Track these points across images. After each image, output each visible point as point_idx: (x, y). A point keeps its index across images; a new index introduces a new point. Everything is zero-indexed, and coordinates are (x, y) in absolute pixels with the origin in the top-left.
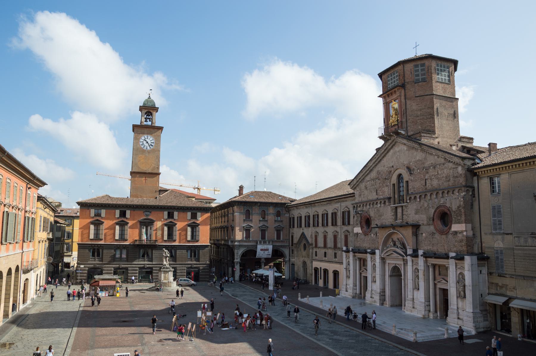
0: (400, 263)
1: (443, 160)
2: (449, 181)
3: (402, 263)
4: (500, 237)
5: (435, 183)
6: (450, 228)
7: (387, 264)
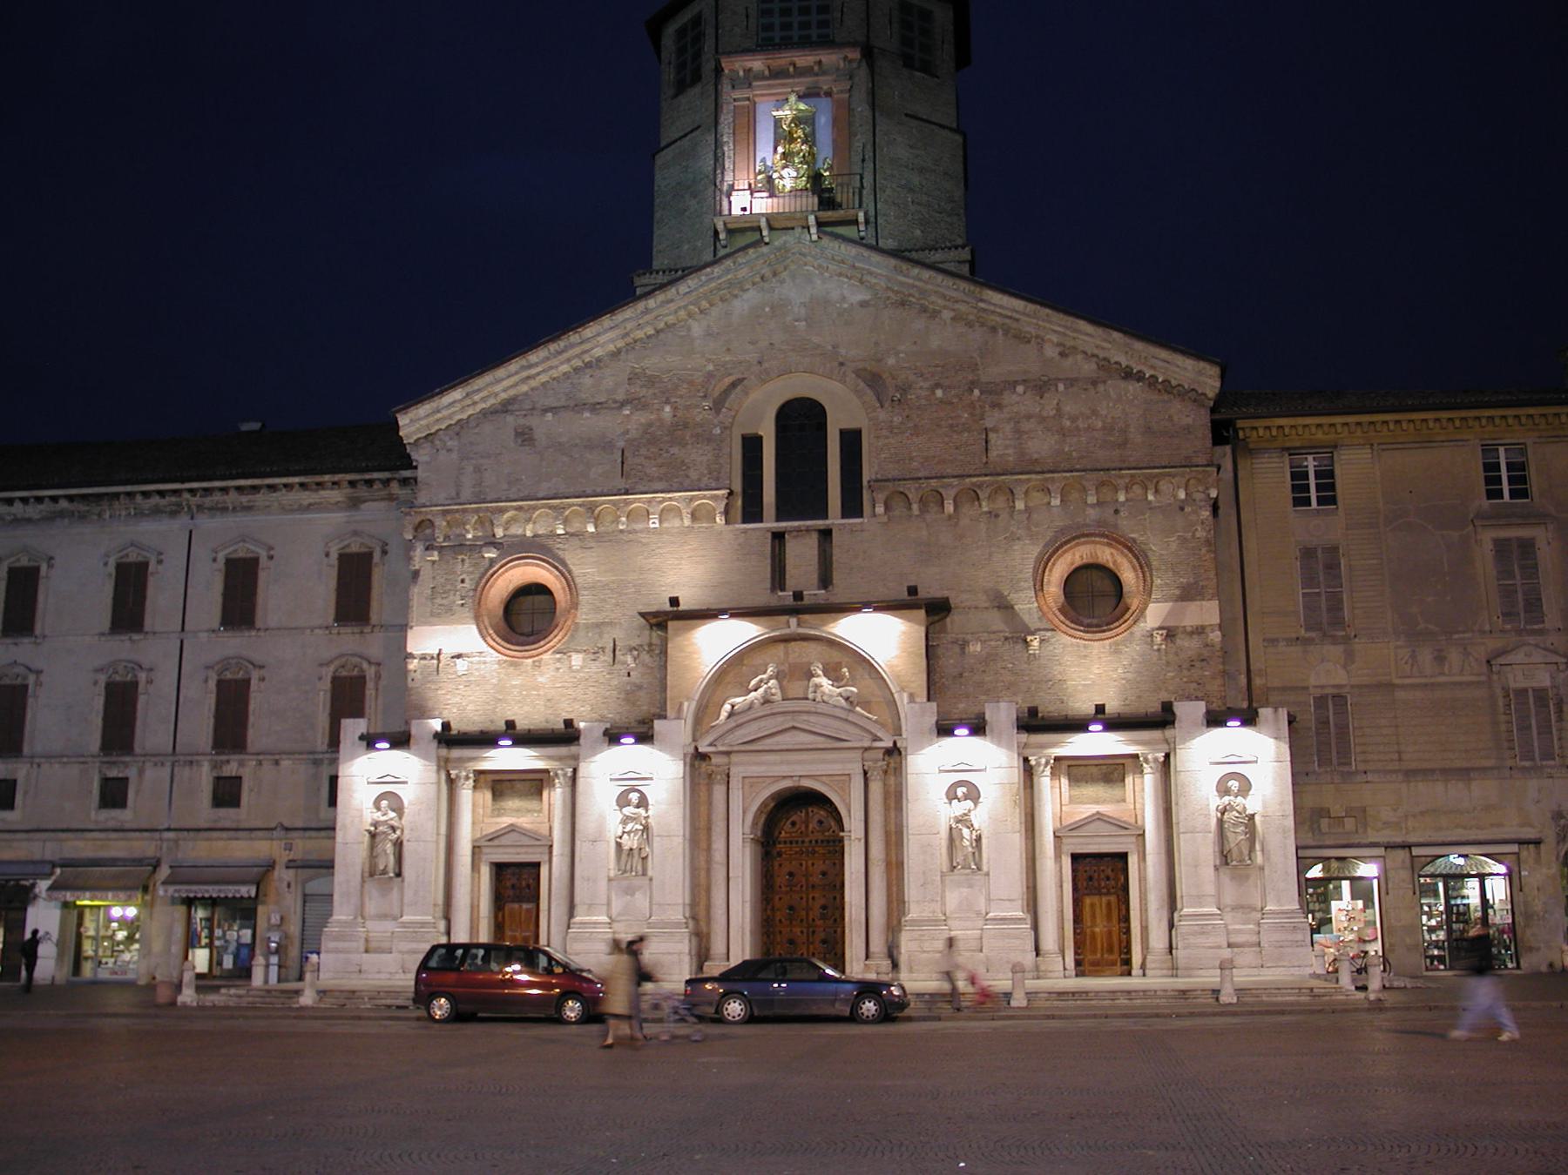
2: (1123, 444)
4: (1336, 651)
5: (1041, 445)
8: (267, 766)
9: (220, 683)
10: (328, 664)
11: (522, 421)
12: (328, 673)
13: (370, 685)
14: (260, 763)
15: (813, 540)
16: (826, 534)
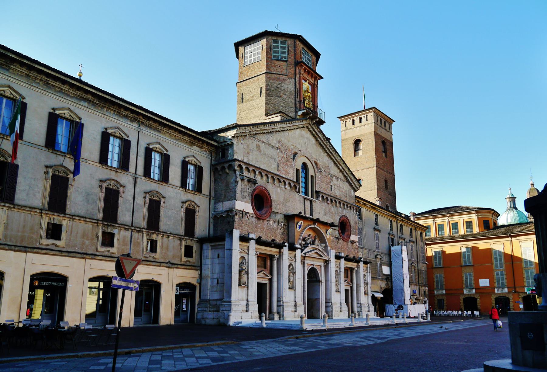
0: (318, 264)
1: (343, 177)
3: (322, 264)
6: (350, 237)
8: (165, 238)
9: (150, 200)
10: (185, 202)
11: (258, 143)
12: (185, 206)
13: (197, 214)
14: (163, 236)
15: (309, 202)
16: (311, 202)
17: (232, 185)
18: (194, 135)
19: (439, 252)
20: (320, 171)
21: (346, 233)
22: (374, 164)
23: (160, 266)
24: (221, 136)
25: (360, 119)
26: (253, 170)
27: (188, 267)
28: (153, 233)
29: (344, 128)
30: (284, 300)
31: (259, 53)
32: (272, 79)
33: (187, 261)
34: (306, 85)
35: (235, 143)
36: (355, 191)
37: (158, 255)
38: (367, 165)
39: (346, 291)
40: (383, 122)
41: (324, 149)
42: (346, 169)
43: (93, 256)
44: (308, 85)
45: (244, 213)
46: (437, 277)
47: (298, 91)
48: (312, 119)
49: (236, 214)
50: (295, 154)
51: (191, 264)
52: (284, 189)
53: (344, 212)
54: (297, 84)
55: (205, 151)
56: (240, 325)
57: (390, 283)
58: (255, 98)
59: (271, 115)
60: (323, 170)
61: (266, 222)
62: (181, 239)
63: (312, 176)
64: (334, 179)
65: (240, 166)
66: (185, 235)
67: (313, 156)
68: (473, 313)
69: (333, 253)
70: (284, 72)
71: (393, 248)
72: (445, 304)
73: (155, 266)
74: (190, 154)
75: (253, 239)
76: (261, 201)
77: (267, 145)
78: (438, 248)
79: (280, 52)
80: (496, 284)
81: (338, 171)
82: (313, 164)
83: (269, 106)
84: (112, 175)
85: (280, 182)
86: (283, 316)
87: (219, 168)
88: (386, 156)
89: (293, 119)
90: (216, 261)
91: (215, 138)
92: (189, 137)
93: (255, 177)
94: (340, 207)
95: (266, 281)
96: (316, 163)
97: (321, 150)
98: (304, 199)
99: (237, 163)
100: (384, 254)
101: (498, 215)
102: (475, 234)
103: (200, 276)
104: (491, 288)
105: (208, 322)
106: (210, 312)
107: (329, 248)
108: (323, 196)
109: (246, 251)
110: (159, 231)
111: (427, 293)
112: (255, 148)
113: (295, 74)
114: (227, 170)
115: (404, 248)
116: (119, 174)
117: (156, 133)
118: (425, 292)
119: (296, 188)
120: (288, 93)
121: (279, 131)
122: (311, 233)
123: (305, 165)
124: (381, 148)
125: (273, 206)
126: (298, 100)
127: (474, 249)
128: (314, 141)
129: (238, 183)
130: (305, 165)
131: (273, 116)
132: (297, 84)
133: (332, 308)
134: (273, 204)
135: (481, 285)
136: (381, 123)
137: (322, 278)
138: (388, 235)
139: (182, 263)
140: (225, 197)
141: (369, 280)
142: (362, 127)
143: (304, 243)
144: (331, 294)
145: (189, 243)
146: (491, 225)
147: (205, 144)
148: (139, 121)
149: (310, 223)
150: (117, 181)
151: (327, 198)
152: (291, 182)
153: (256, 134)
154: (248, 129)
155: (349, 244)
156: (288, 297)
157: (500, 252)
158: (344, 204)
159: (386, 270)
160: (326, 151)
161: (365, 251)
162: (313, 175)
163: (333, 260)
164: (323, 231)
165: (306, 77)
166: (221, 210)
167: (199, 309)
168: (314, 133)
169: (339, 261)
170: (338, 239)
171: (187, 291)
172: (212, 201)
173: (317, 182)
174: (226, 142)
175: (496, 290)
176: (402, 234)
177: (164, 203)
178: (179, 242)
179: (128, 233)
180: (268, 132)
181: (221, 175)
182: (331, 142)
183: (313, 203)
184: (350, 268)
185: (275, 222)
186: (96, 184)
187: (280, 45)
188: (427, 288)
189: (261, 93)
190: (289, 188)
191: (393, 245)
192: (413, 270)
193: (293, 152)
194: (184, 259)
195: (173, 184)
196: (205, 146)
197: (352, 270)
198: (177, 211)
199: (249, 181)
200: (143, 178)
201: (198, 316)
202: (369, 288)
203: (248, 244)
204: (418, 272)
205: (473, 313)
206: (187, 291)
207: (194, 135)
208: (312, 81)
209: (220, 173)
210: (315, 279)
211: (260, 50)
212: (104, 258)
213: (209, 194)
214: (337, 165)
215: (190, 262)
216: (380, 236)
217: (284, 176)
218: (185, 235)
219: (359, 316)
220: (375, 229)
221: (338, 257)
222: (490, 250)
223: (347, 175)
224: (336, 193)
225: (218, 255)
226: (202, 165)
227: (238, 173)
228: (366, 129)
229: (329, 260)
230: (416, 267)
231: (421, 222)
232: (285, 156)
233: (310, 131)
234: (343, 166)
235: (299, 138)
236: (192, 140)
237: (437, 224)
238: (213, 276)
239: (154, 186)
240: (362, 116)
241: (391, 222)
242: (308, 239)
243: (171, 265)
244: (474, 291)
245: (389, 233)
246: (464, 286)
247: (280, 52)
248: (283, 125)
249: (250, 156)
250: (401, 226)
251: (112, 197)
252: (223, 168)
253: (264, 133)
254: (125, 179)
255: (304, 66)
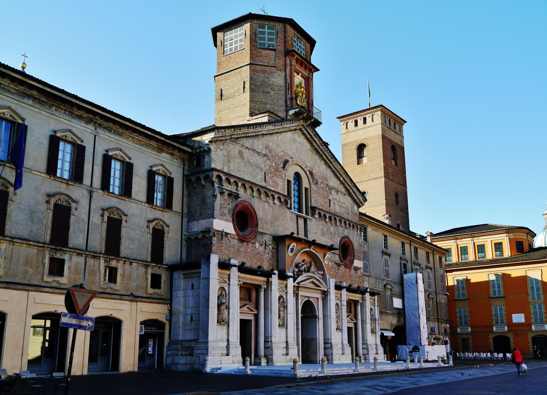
0: (315, 295)
1: (343, 190)
3: (319, 296)
4: (367, 278)
6: (353, 263)
7: (300, 297)
11: (240, 149)
12: (152, 225)
13: (166, 235)
14: (124, 263)
15: (303, 220)
16: (305, 220)
17: (208, 200)
18: (163, 139)
19: (462, 281)
20: (316, 183)
21: (348, 258)
22: (382, 173)
23: (121, 299)
24: (195, 141)
25: (365, 119)
26: (235, 182)
27: (155, 301)
28: (112, 259)
29: (345, 131)
30: (273, 340)
31: (241, 40)
32: (258, 71)
33: (154, 293)
34: (298, 79)
35: (213, 149)
36: (359, 206)
37: (118, 286)
38: (374, 176)
39: (349, 329)
40: (392, 123)
41: (321, 156)
42: (348, 180)
43: (39, 288)
44: (301, 78)
45: (224, 233)
46: (460, 312)
47: (289, 85)
48: (306, 119)
49: (214, 236)
50: (286, 162)
51: (158, 297)
52: (272, 204)
53: (346, 232)
54: (288, 78)
55: (177, 159)
56: (219, 371)
57: (402, 319)
58: (237, 94)
59: (257, 115)
60: (320, 181)
61: (250, 245)
62: (146, 266)
63: (306, 189)
64: (333, 192)
65: (219, 177)
66: (152, 261)
67: (308, 164)
68: (505, 355)
69: (332, 282)
70: (272, 63)
71: (405, 276)
72: (471, 345)
73: (114, 299)
74: (159, 162)
75: (235, 266)
76: (244, 219)
77: (251, 152)
78: (461, 275)
79: (266, 39)
80: (533, 320)
81: (338, 182)
82: (308, 173)
83: (254, 104)
84: (63, 188)
85: (267, 195)
86: (272, 360)
87: (193, 179)
88: (396, 164)
89: (283, 120)
90: (190, 293)
91: (188, 143)
92: (156, 142)
93: (237, 190)
94: (341, 226)
95: (251, 317)
96: (311, 173)
97: (317, 157)
98: (297, 216)
99: (215, 174)
100: (394, 283)
101: (534, 235)
102: (506, 258)
103: (170, 311)
104: (527, 324)
105: (180, 368)
106: (182, 355)
107: (328, 276)
108: (319, 214)
109: (227, 280)
110: (119, 257)
111: (448, 331)
112: (237, 155)
113: (285, 65)
114: (203, 182)
115: (420, 276)
116: (71, 187)
117: (116, 137)
118: (445, 330)
119: (287, 203)
120: (276, 88)
121: (266, 134)
122: (306, 258)
123: (297, 176)
124: (391, 154)
125: (259, 225)
126: (289, 96)
127: (505, 276)
128: (308, 146)
129: (216, 198)
130: (297, 176)
131: (259, 116)
132: (288, 78)
133: (332, 350)
134: (259, 223)
135: (514, 321)
136: (390, 125)
137: (320, 313)
138: (399, 261)
139: (148, 296)
140: (201, 215)
141: (377, 315)
142: (366, 129)
143: (297, 270)
144: (331, 333)
145: (157, 271)
146: (526, 247)
147: (176, 151)
148: (95, 123)
149: (304, 246)
150: (68, 196)
151: (325, 215)
152: (281, 196)
153: (238, 138)
154: (228, 132)
155: (352, 271)
156: (278, 336)
157: (537, 280)
158: (345, 223)
159: (397, 303)
160: (323, 158)
161: (372, 280)
162: (308, 187)
163: (333, 291)
164: (320, 256)
165: (298, 69)
166: (196, 230)
167: (169, 353)
168: (309, 136)
169: (340, 292)
170: (338, 265)
171: (154, 330)
172: (185, 220)
173: (312, 195)
174: (201, 147)
175: (533, 328)
176: (417, 259)
177: (126, 221)
178: (145, 270)
179: (81, 260)
180: (253, 136)
181: (195, 188)
182: (329, 147)
183: (308, 222)
184: (353, 300)
185: (261, 245)
186: (42, 199)
187: (267, 31)
188: (448, 325)
189: (244, 88)
190: (278, 203)
191: (406, 272)
192: (431, 303)
193: (283, 159)
194: (150, 291)
195: (137, 199)
196: (176, 152)
197: (356, 302)
198: (142, 232)
199: (230, 195)
200: (100, 191)
201: (167, 361)
202: (377, 325)
203: (228, 272)
204: (437, 305)
205: (505, 355)
206: (154, 330)
207: (163, 139)
208: (306, 74)
209: (195, 185)
210: (310, 314)
211: (243, 37)
212: (51, 290)
213: (181, 212)
214: (336, 176)
215: (157, 294)
216: (389, 262)
217: (272, 189)
218: (152, 261)
219: (365, 359)
220: (384, 253)
221: (338, 288)
222: (524, 279)
223: (348, 188)
224: (336, 208)
225: (193, 285)
226: (172, 176)
227: (216, 185)
228: (372, 131)
229: (327, 291)
230: (435, 299)
231: (439, 244)
232: (274, 165)
233: (304, 134)
234: (344, 176)
235: (290, 142)
236: (161, 145)
237: (459, 246)
238: (186, 311)
239: (114, 202)
240: (367, 116)
241: (403, 244)
242: (303, 265)
243: (134, 298)
244: (506, 328)
245: (401, 258)
246: (494, 322)
247: (266, 39)
248: (271, 127)
249: (231, 164)
250: (416, 249)
251: (62, 215)
252: (199, 179)
253: (248, 137)
254: (78, 193)
255: (297, 56)
